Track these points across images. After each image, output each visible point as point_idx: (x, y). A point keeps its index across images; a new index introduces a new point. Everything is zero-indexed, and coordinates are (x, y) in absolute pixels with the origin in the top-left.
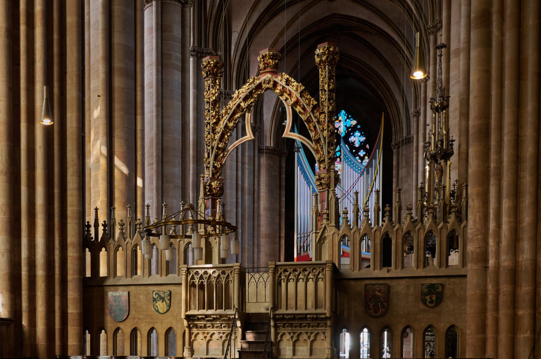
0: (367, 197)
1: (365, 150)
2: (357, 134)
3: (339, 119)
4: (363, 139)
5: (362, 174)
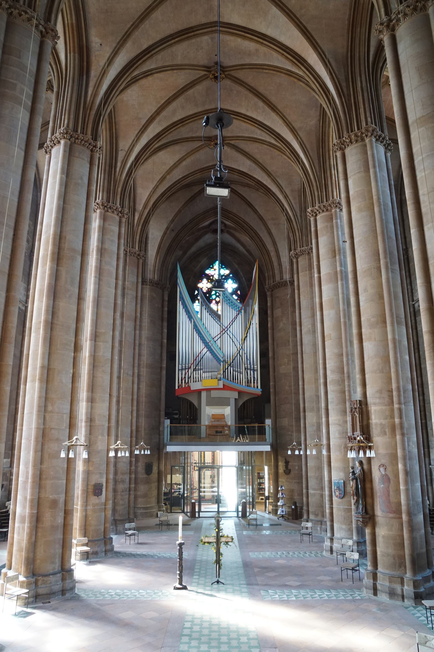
0: (246, 333)
1: (237, 295)
2: (230, 281)
4: (235, 286)
5: (240, 311)
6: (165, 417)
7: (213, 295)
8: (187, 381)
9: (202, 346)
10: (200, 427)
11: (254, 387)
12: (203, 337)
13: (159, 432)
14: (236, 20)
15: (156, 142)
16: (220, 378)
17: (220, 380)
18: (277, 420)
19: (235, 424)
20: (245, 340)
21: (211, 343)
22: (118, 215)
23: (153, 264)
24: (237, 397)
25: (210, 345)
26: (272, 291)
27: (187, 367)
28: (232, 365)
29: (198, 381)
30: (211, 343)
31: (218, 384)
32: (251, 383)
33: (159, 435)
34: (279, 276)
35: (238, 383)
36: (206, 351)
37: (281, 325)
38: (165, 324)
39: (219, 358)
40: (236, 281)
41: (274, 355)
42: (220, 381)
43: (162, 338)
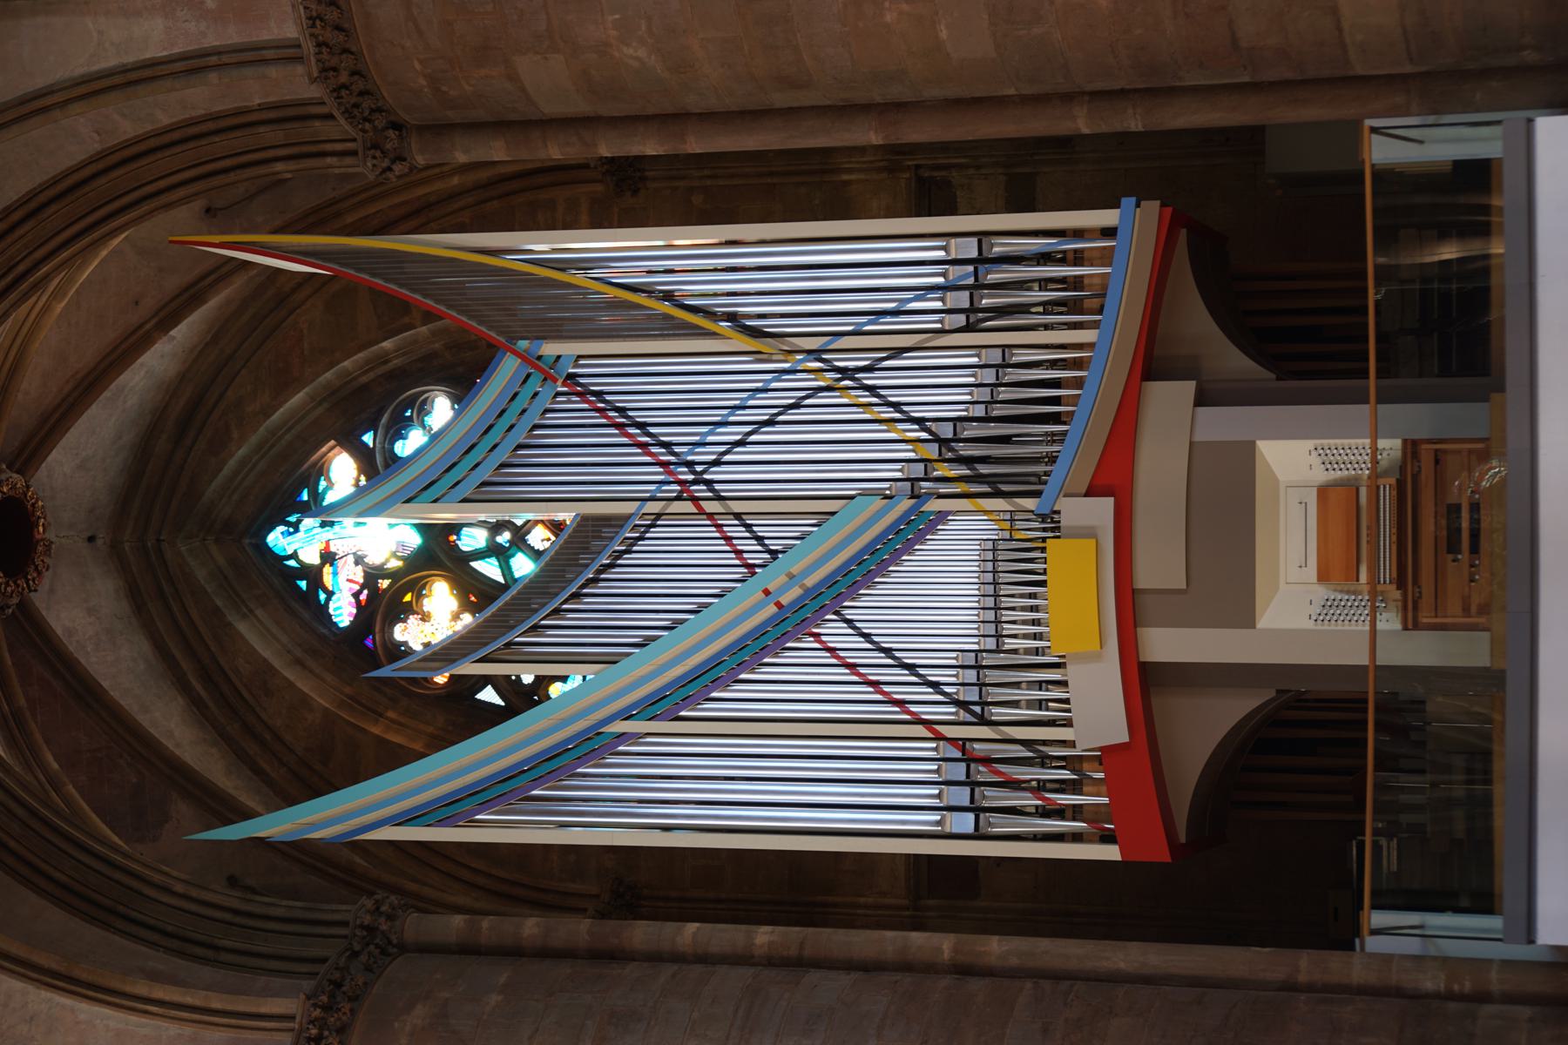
3: (316, 561)
6: (1351, 948)
7: (506, 569)
8: (1065, 775)
9: (804, 651)
10: (1379, 669)
11: (1105, 257)
12: (739, 646)
13: (1462, 998)
16: (1043, 518)
17: (1051, 522)
18: (1360, 70)
19: (1362, 399)
20: (756, 333)
21: (784, 589)
23: (188, 1030)
24: (1190, 387)
25: (795, 593)
26: (397, 126)
27: (959, 771)
28: (946, 431)
29: (1063, 684)
30: (784, 589)
31: (1089, 533)
32: (1077, 283)
33: (1482, 997)
34: (273, 72)
35: (1078, 383)
36: (842, 628)
37: (635, 53)
38: (641, 933)
39: (894, 529)
40: (410, 403)
41: (866, 108)
42: (1065, 520)
43: (742, 959)
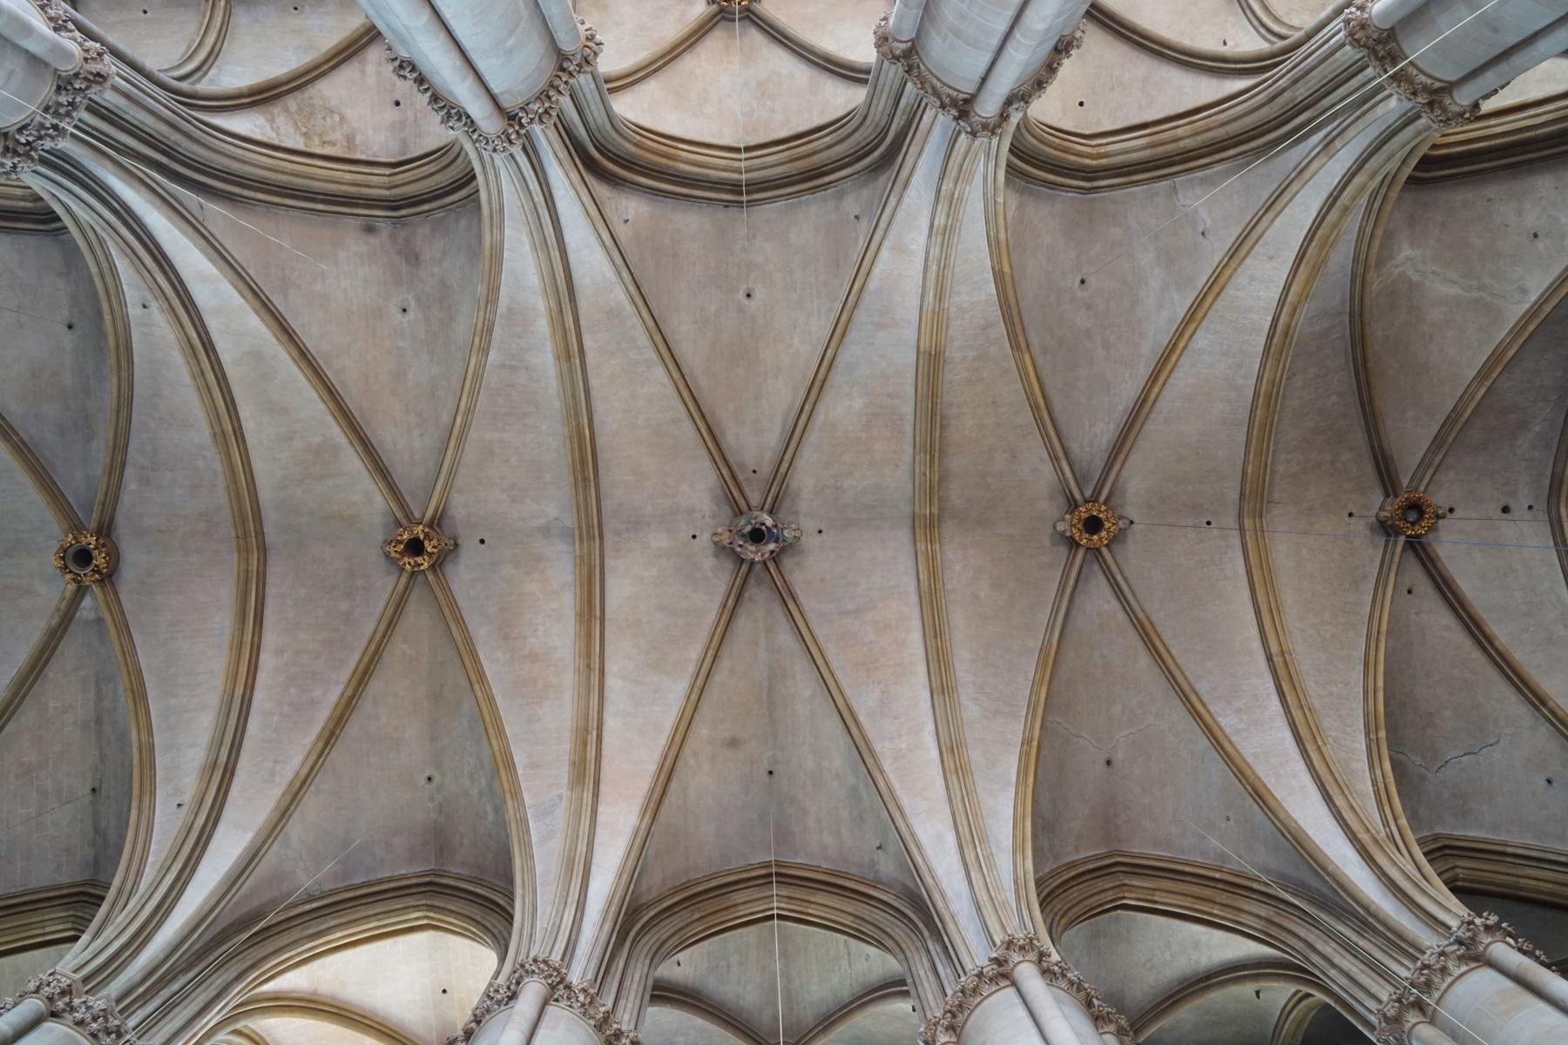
14: (620, 591)
15: (194, 335)
22: (25, 127)
